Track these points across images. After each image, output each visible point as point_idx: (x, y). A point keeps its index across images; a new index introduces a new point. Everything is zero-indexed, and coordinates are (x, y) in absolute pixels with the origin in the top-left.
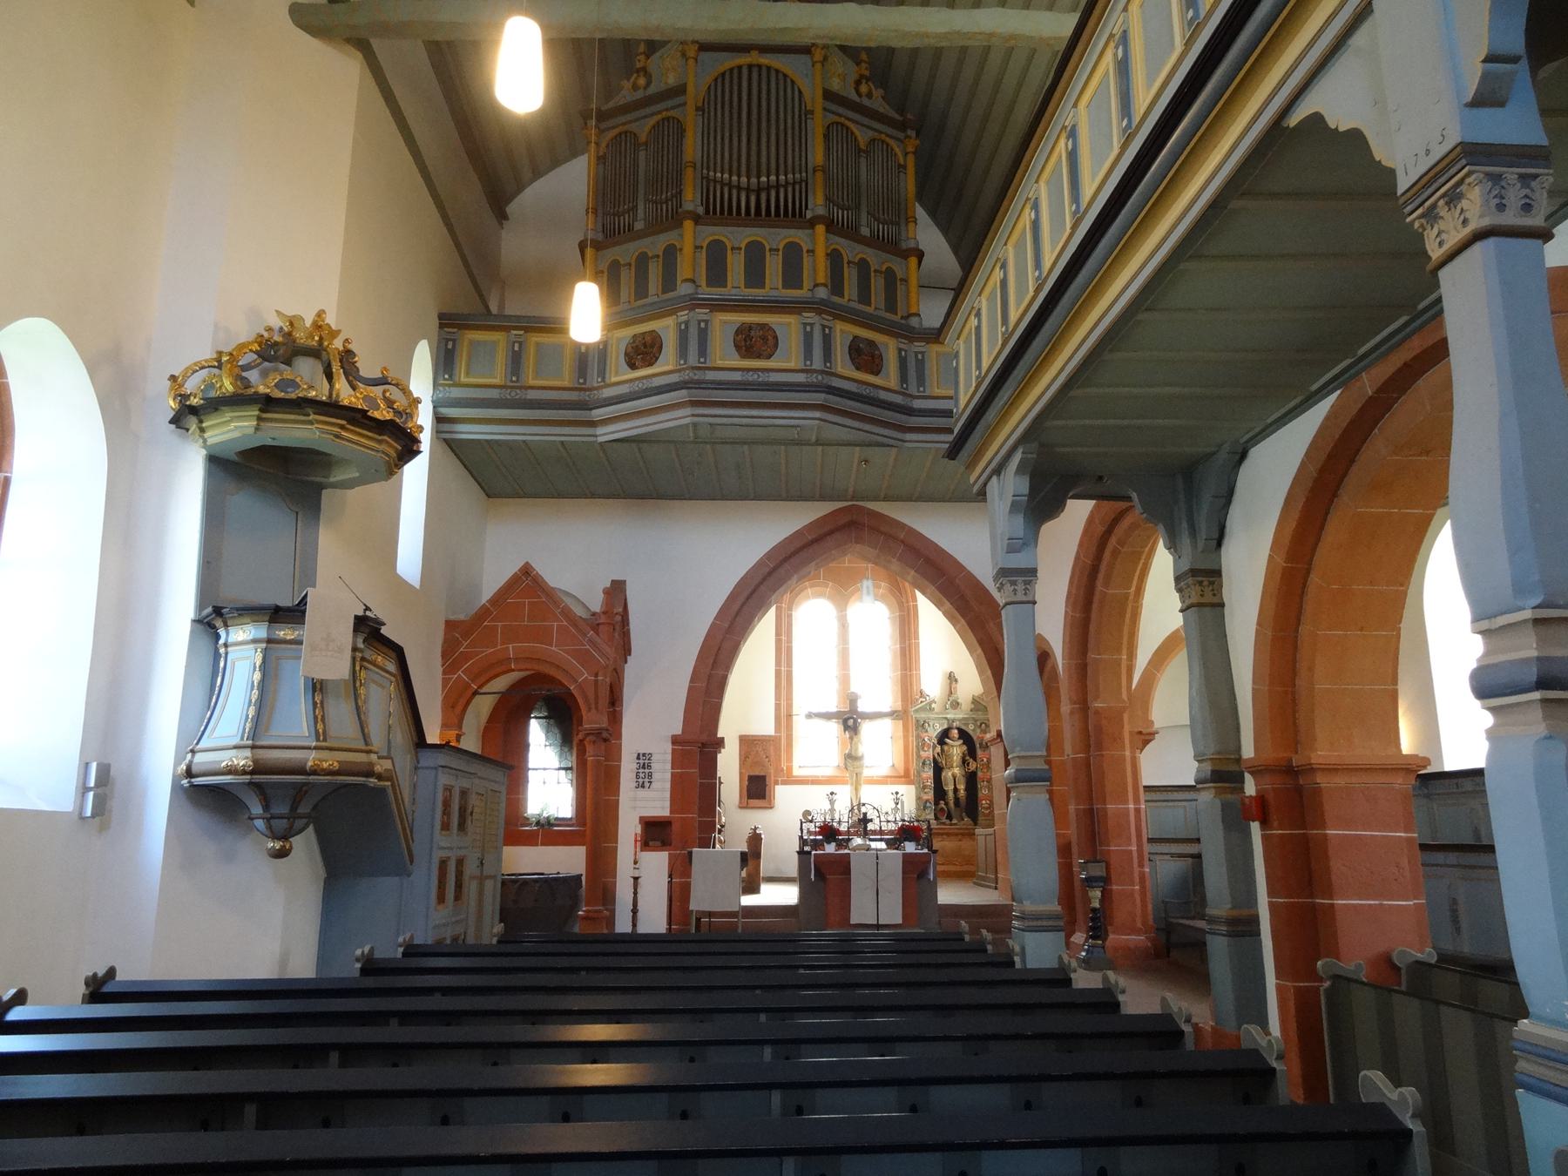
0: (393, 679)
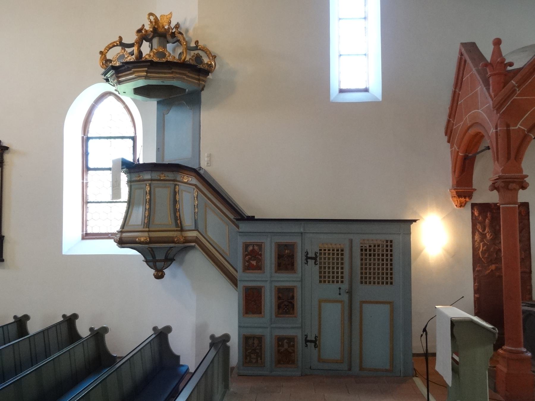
0: (194, 187)
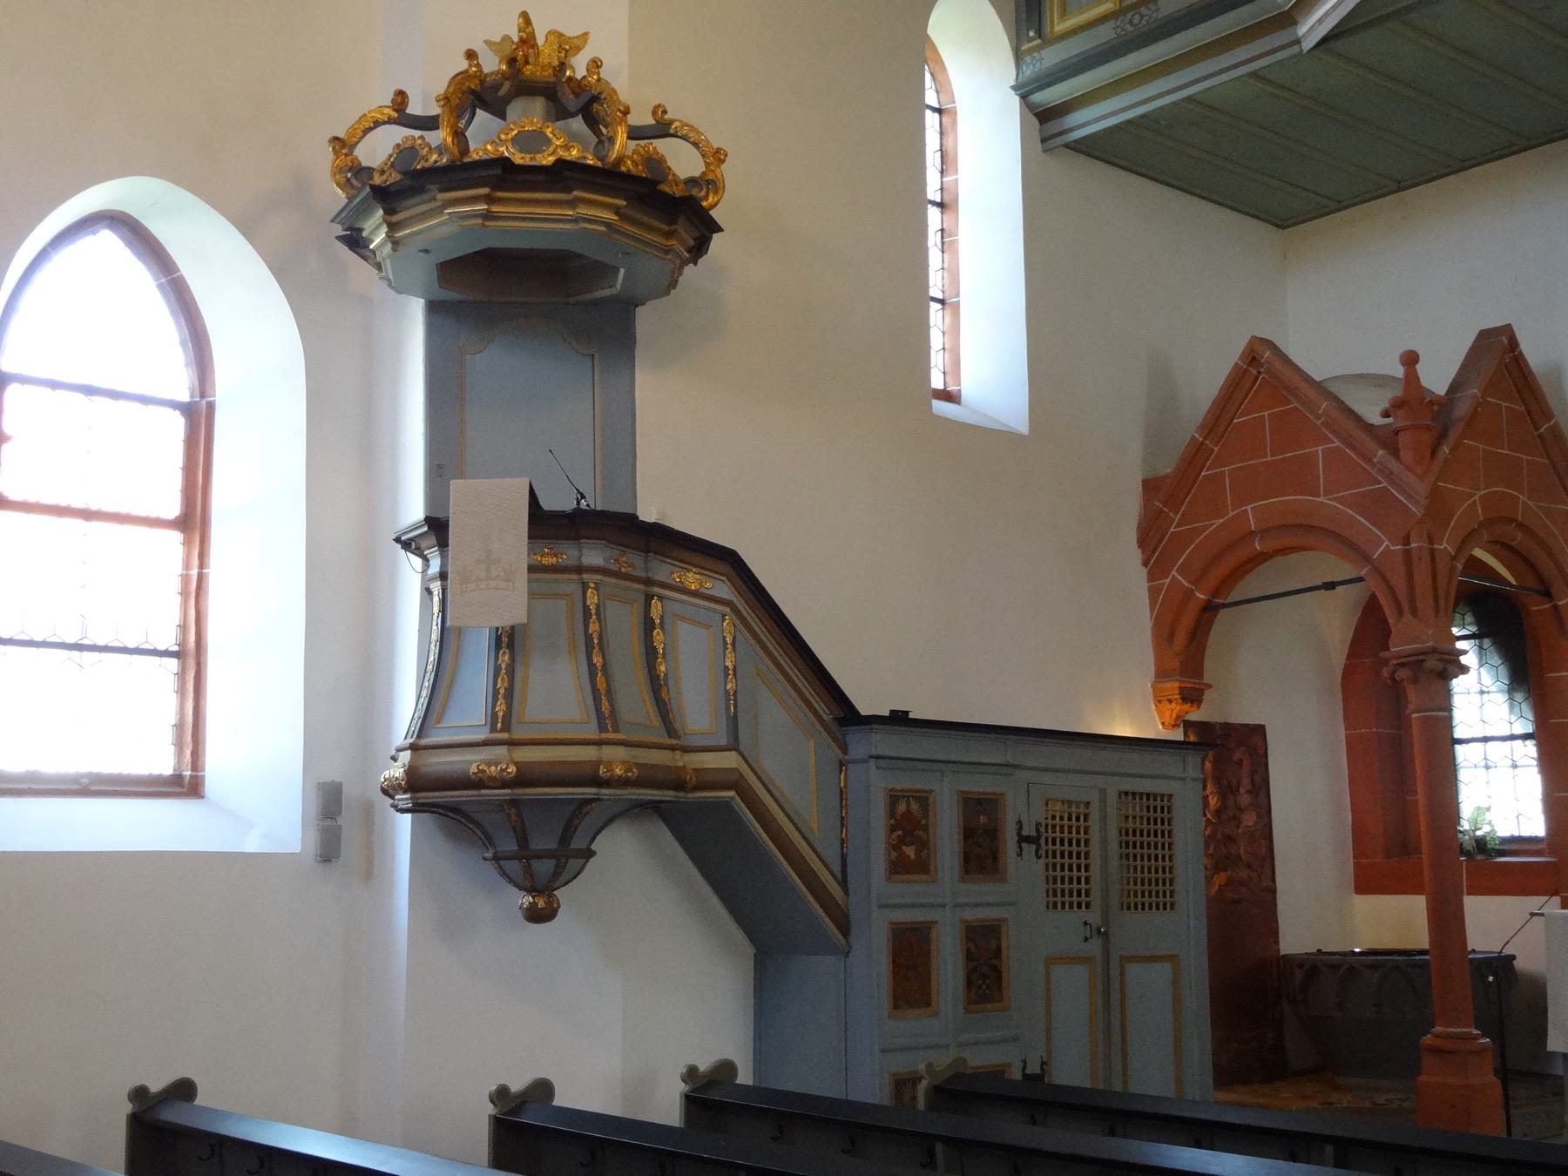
0: (727, 610)
